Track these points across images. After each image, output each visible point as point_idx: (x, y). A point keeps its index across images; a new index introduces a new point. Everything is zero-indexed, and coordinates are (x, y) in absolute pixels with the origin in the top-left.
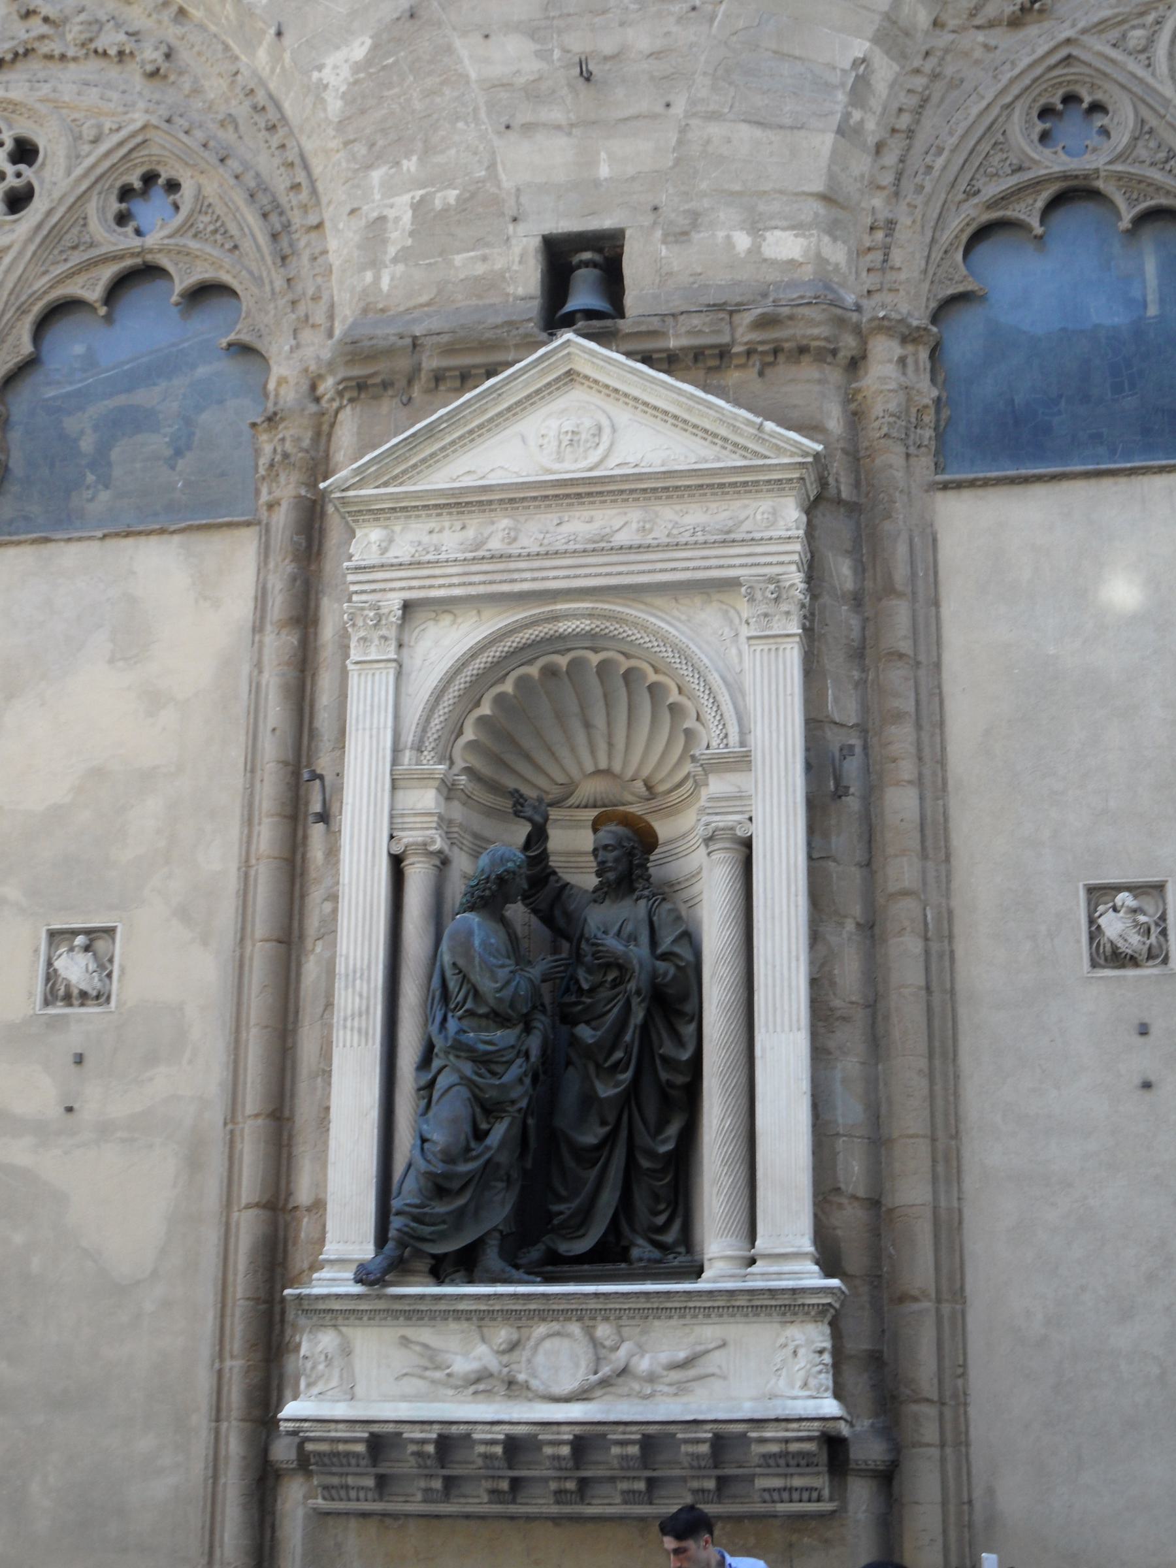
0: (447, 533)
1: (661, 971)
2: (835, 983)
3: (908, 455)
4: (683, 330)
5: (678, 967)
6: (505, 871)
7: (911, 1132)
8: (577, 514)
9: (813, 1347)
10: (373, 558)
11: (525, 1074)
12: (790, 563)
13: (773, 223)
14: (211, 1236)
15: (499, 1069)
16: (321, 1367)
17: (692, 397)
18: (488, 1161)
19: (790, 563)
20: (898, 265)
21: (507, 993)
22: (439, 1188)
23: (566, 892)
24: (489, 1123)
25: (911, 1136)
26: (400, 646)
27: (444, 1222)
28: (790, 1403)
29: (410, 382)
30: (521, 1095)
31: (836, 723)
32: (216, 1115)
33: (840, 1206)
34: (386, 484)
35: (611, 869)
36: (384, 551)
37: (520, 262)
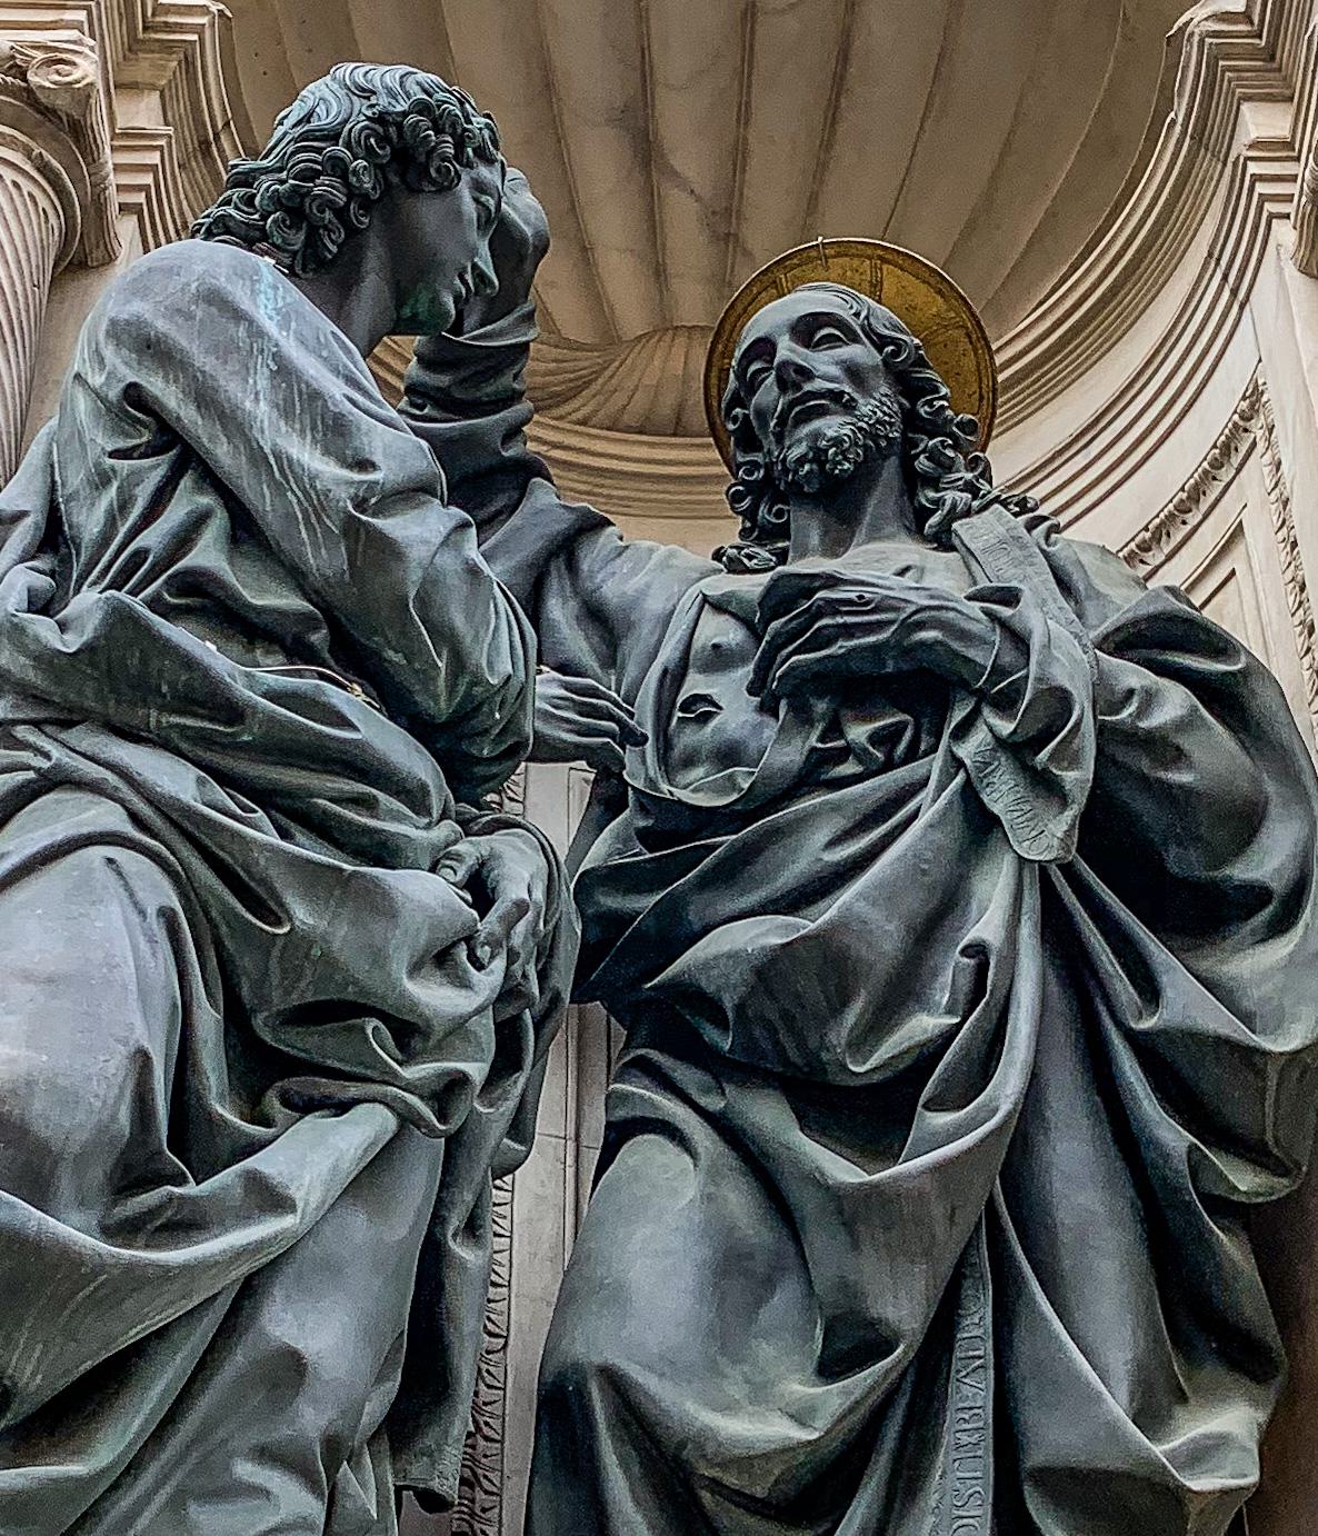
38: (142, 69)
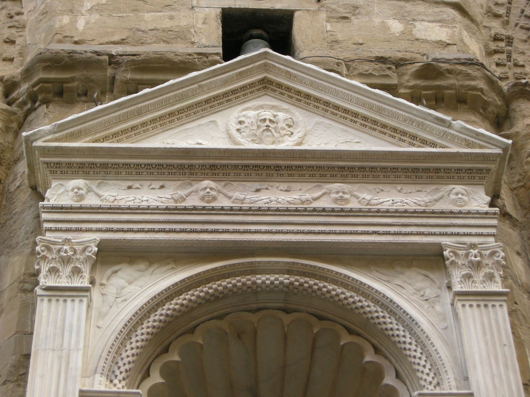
4: (356, 72)
8: (277, 184)
12: (488, 235)
13: (420, 17)
19: (488, 235)
20: (521, 63)
26: (92, 282)
36: (81, 197)
37: (204, 23)
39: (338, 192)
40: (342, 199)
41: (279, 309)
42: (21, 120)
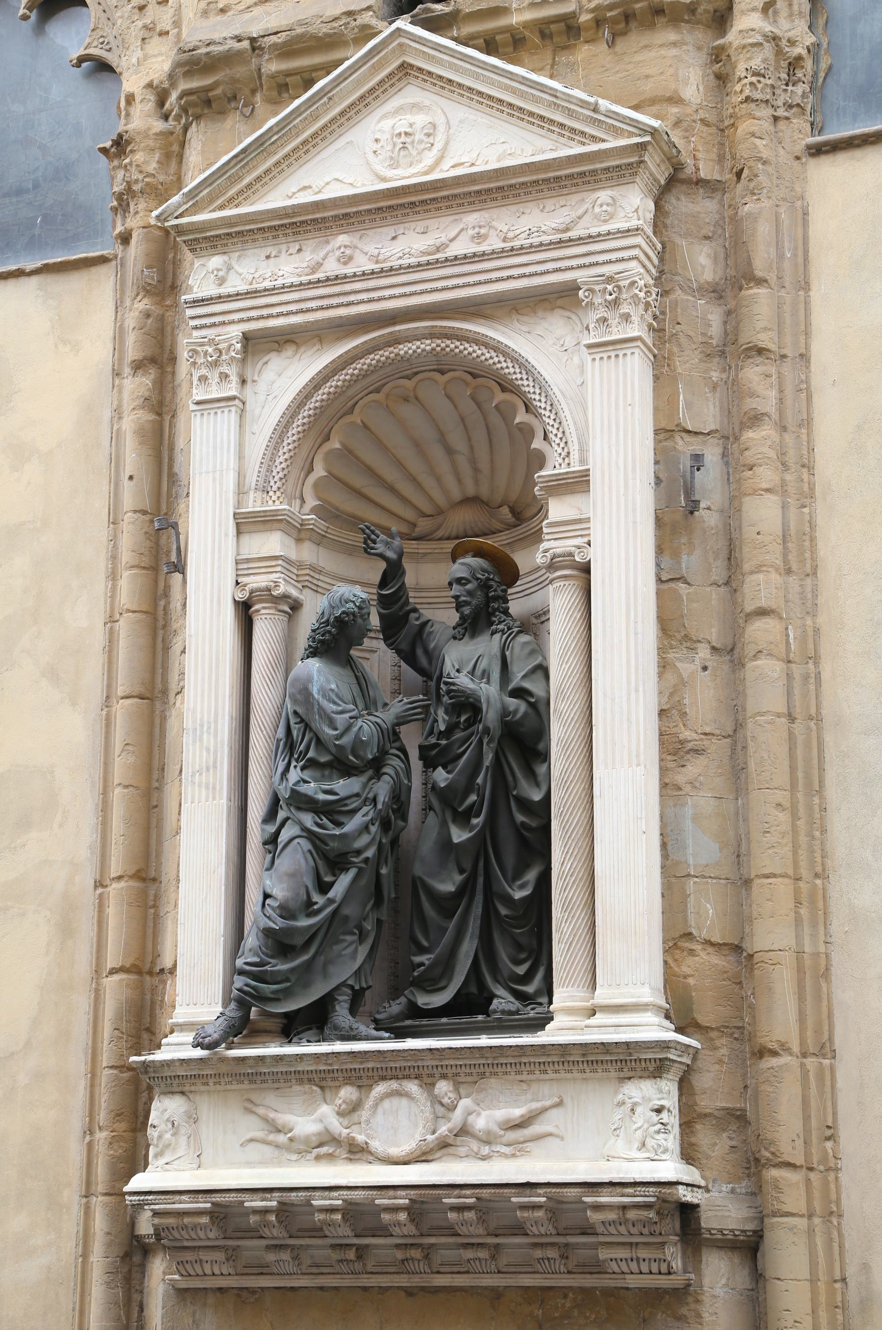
0: (283, 255)
1: (511, 709)
2: (685, 713)
3: (776, 119)
5: (529, 703)
6: (343, 612)
7: (766, 871)
8: (413, 225)
9: (651, 1105)
10: (211, 290)
11: (372, 822)
14: (82, 1002)
15: (342, 819)
16: (168, 1136)
17: (524, 81)
18: (335, 912)
21: (346, 740)
22: (279, 943)
23: (428, 629)
24: (334, 875)
25: (767, 876)
26: (244, 382)
27: (287, 980)
28: (625, 1165)
29: (254, 92)
30: (366, 846)
31: (689, 432)
32: (87, 878)
33: (692, 952)
34: (222, 207)
35: (467, 603)
36: (222, 281)
38: (303, 535)
39: (474, 228)
40: (479, 236)
41: (434, 370)
42: (181, 138)
